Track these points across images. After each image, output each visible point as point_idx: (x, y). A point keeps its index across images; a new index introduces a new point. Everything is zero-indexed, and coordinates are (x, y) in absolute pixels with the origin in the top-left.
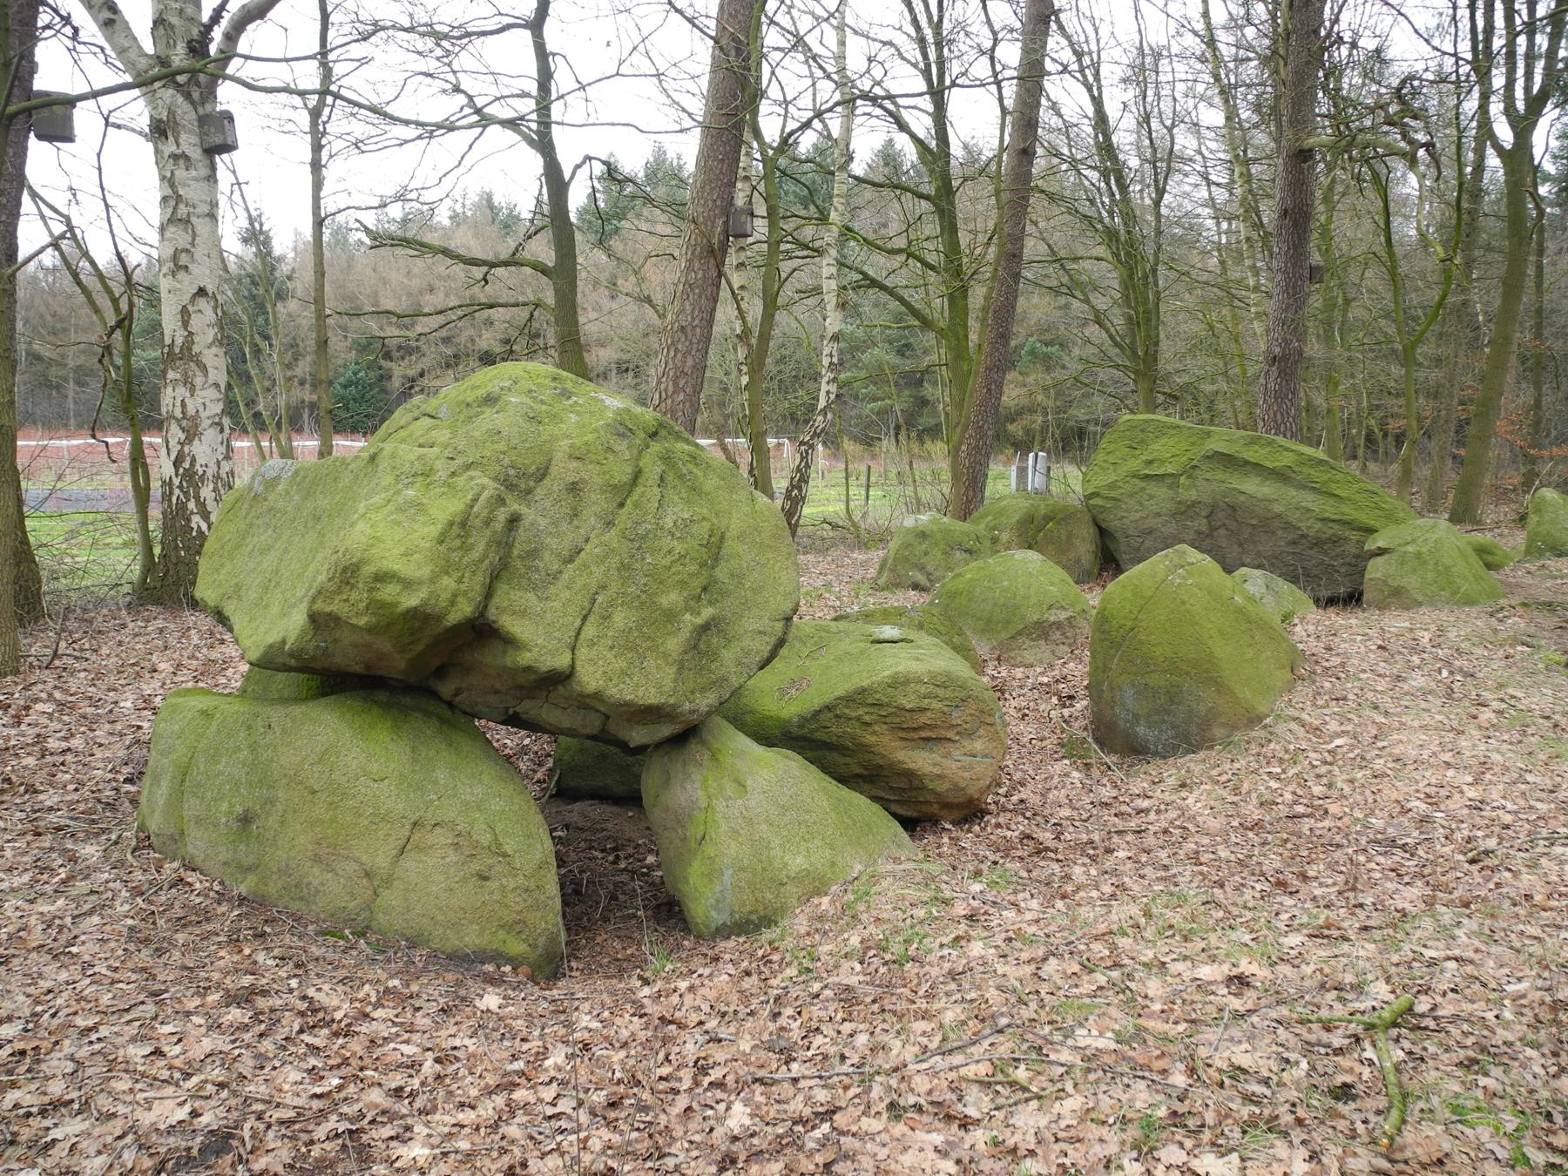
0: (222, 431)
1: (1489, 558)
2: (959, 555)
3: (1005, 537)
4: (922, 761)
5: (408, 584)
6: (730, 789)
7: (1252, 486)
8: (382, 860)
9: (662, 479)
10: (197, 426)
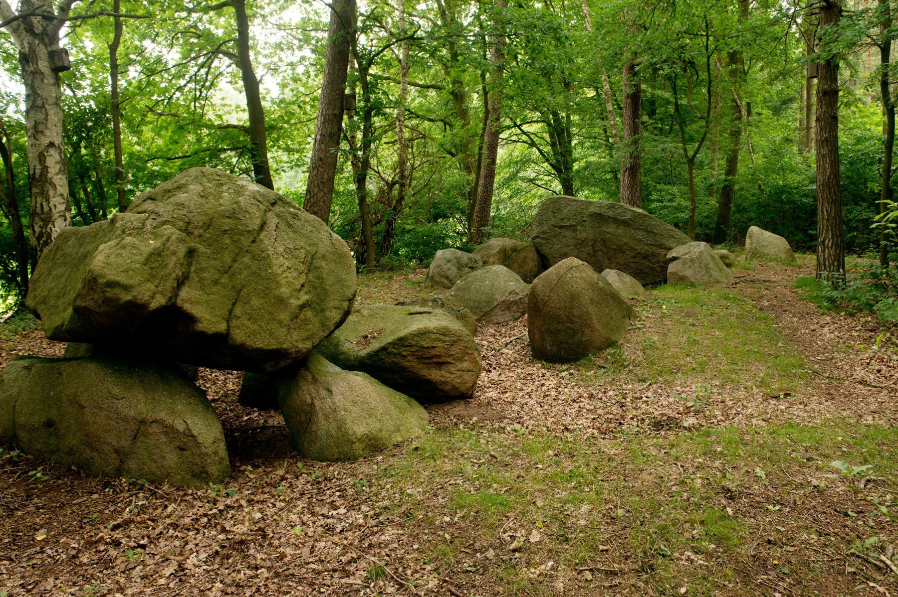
0: (65, 220)
1: (727, 261)
2: (467, 270)
3: (491, 260)
4: (435, 375)
5: (126, 288)
6: (324, 393)
7: (611, 229)
8: (125, 443)
9: (277, 227)
10: (51, 217)
